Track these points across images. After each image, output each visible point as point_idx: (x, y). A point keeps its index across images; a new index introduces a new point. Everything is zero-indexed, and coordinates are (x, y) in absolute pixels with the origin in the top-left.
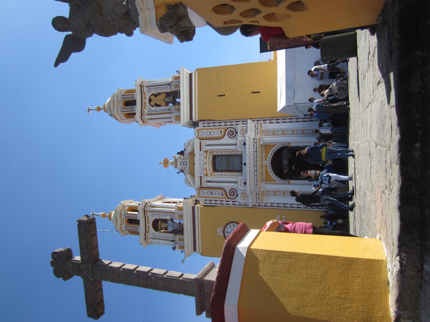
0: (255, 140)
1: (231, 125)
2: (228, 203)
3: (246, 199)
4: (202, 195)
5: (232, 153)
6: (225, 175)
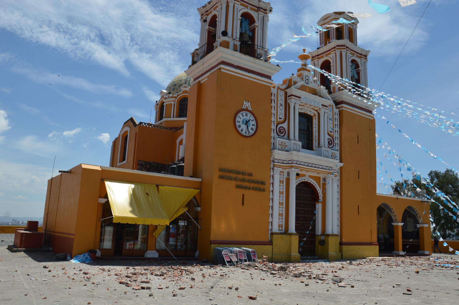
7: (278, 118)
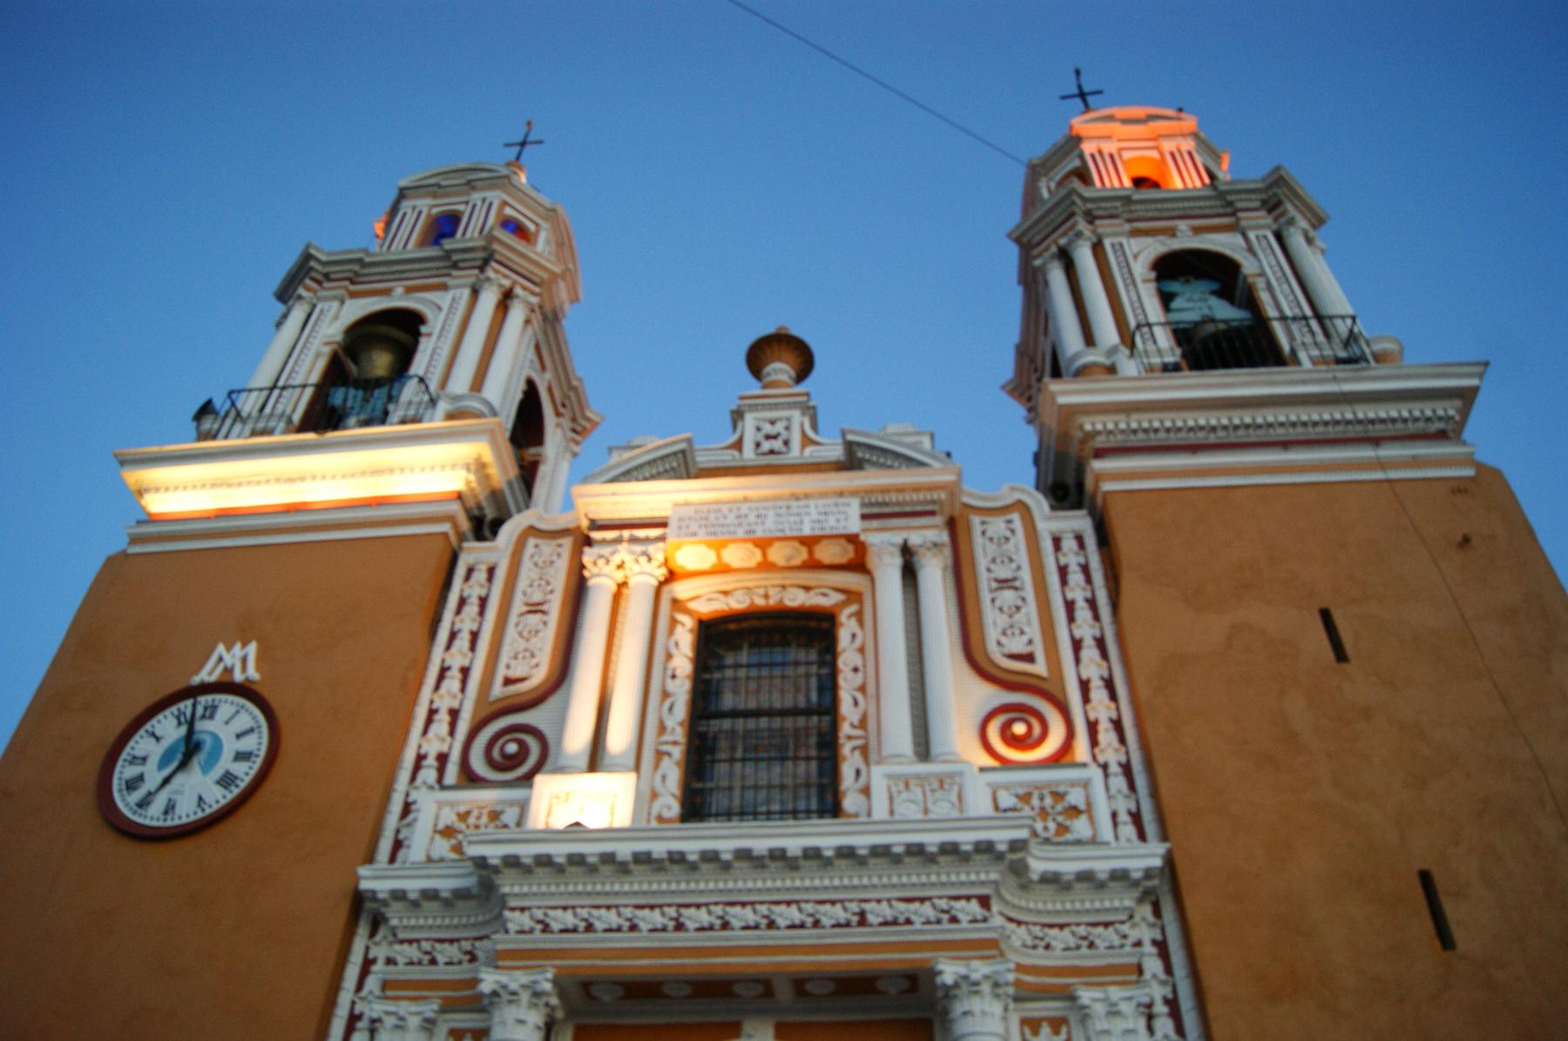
0: (974, 906)
1: (1092, 727)
2: (443, 718)
6: (666, 694)
7: (499, 680)
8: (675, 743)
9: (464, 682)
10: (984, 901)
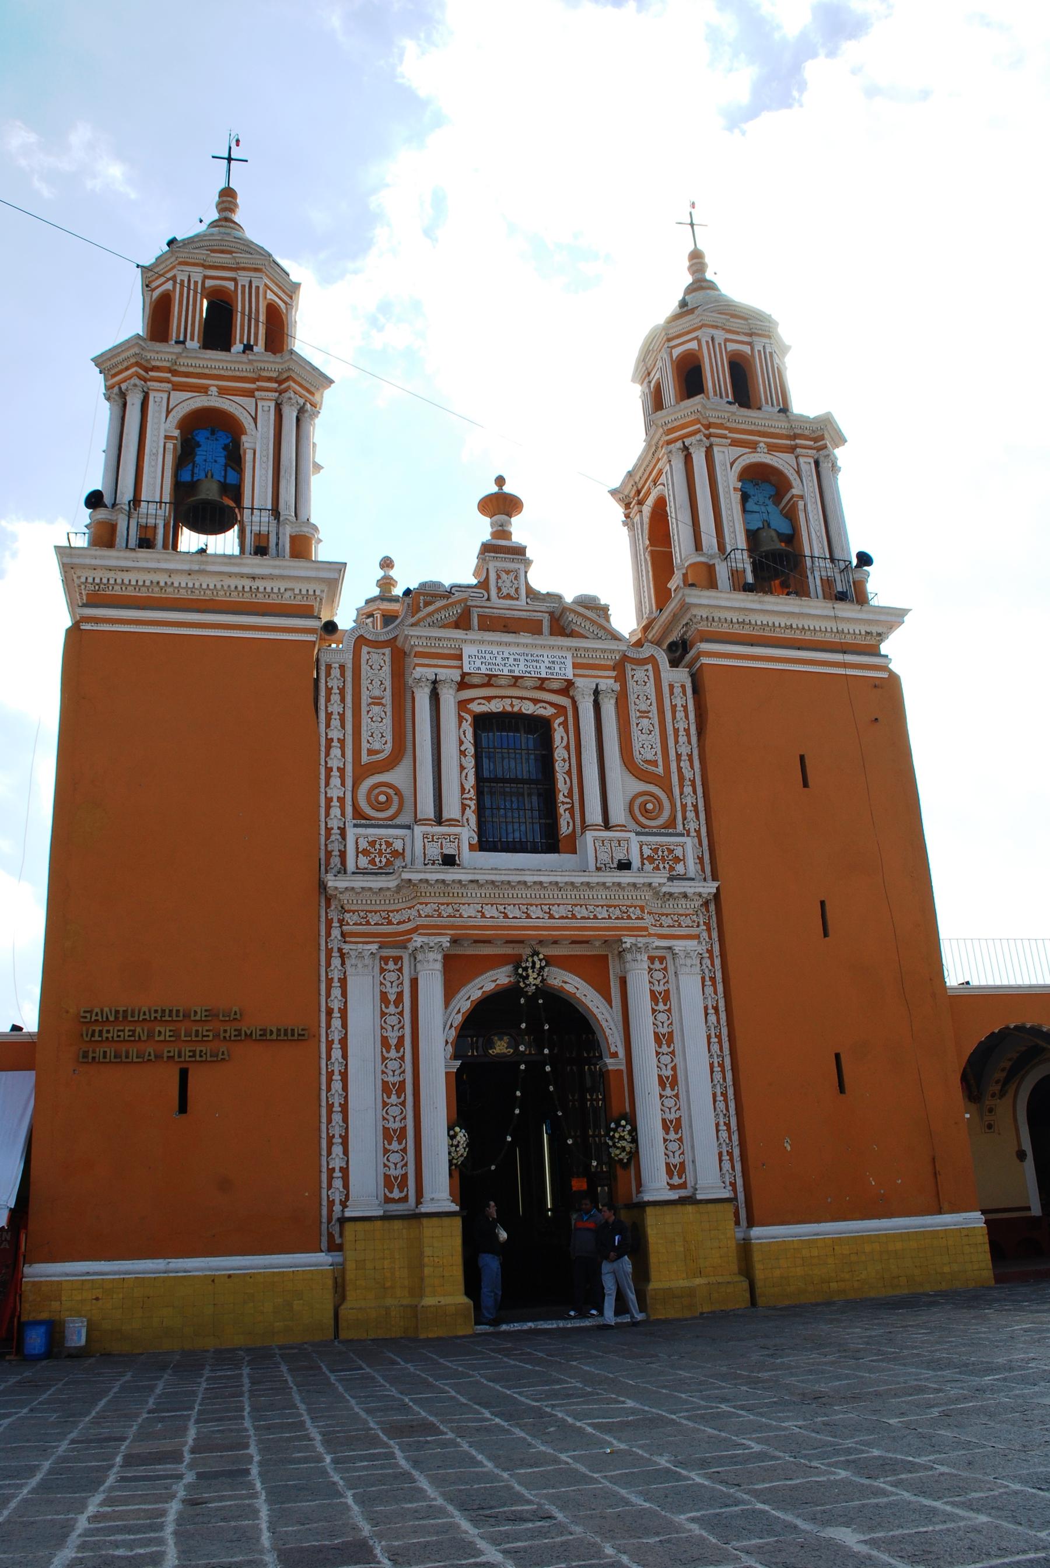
0: (638, 911)
3: (363, 861)
4: (364, 656)
5: (561, 810)
8: (471, 799)
9: (343, 748)
10: (642, 909)
